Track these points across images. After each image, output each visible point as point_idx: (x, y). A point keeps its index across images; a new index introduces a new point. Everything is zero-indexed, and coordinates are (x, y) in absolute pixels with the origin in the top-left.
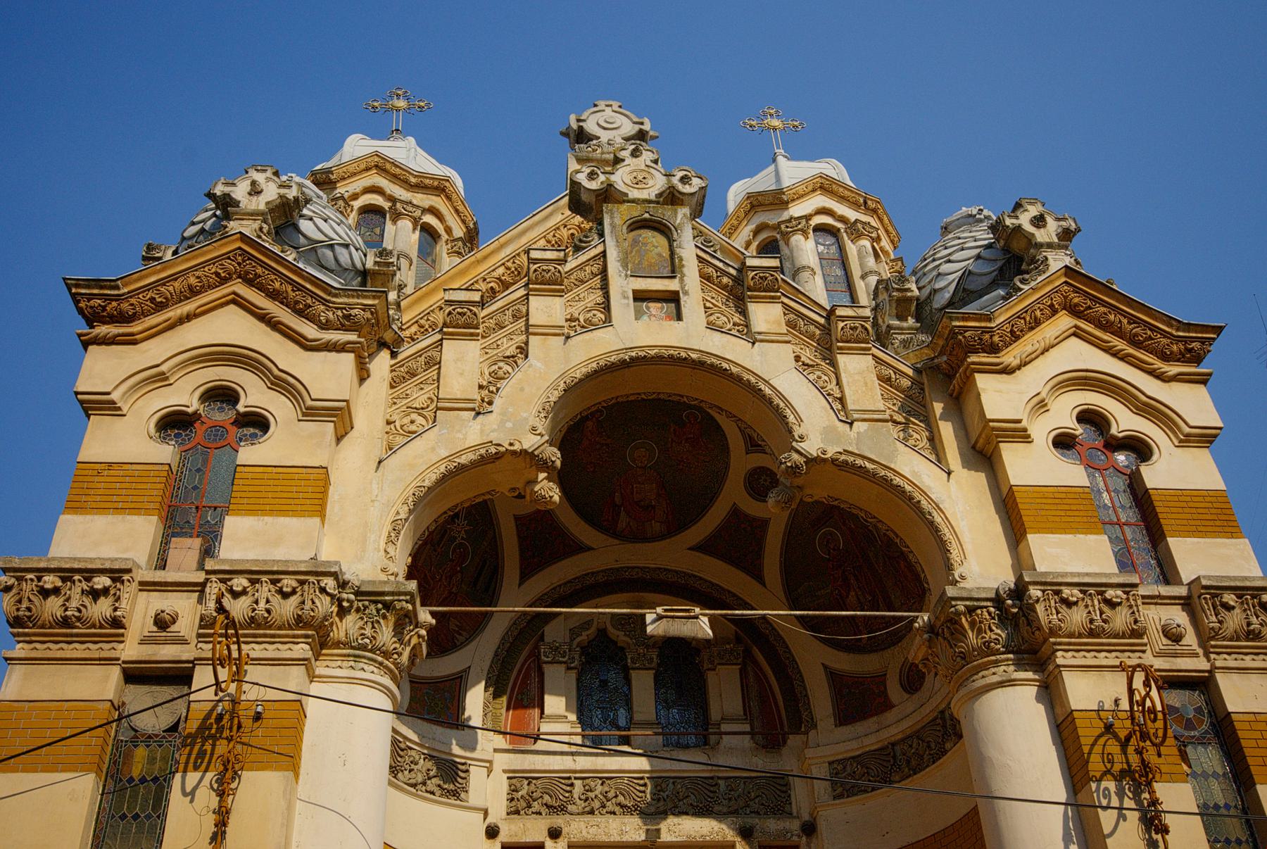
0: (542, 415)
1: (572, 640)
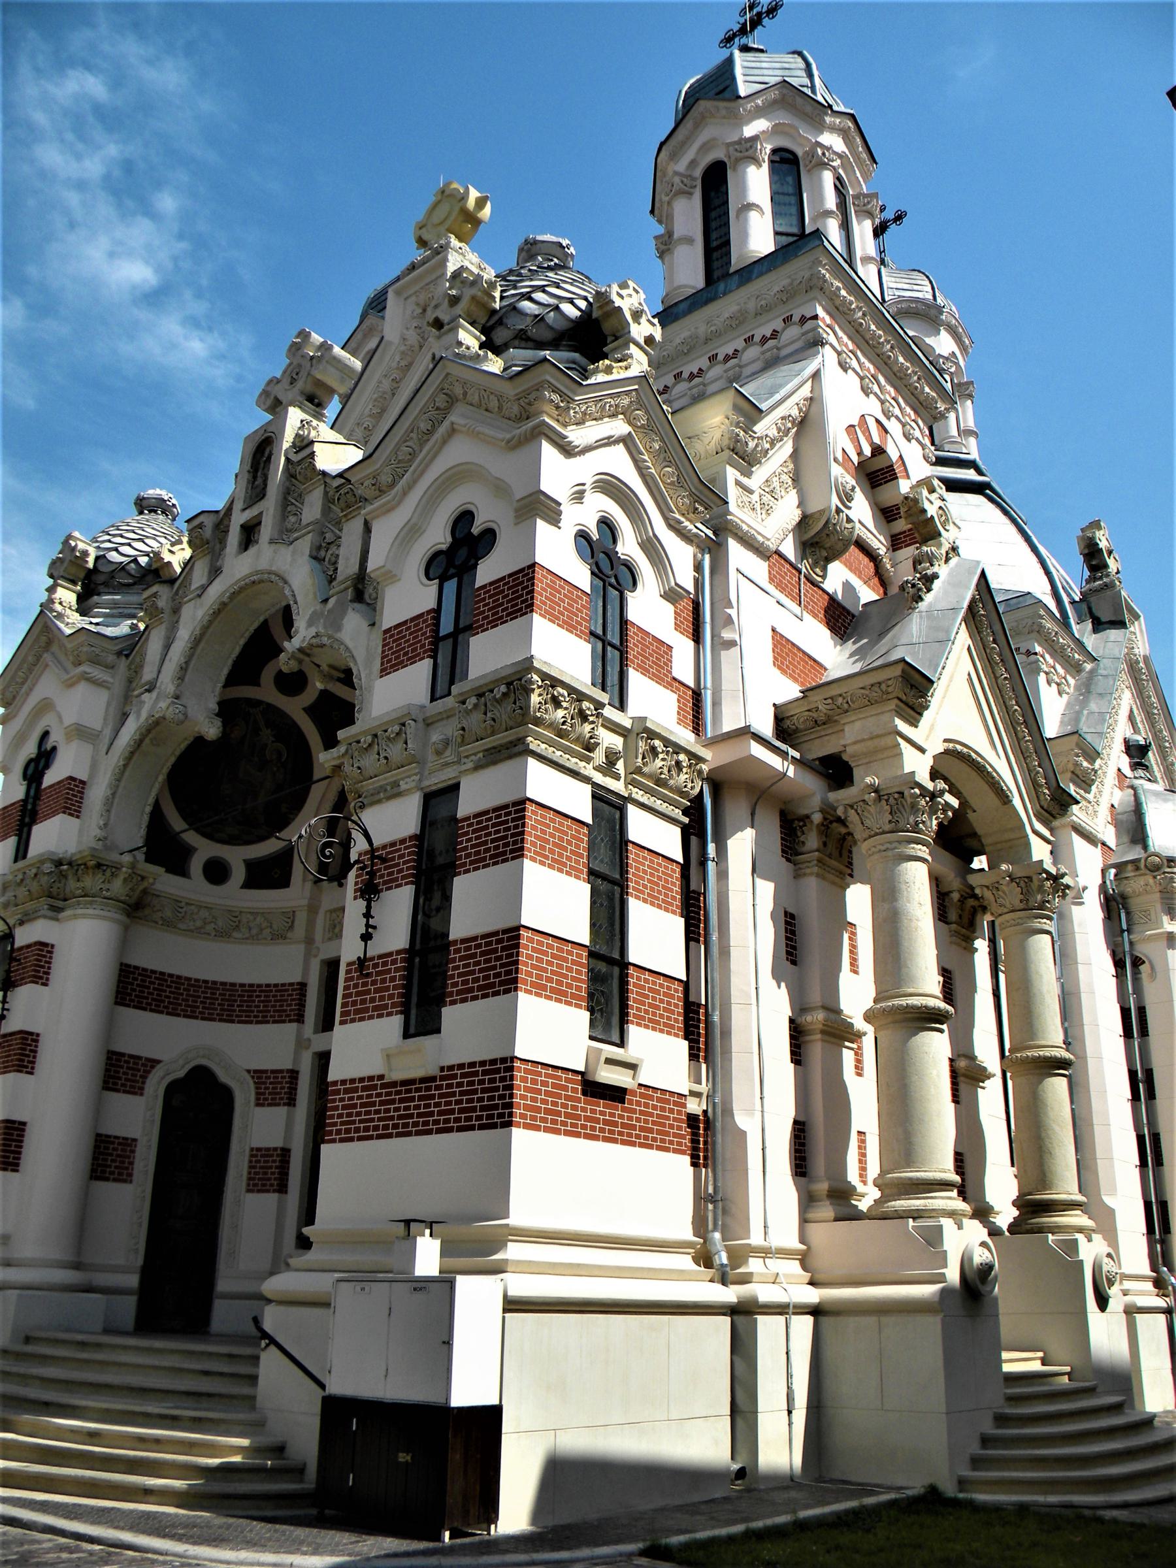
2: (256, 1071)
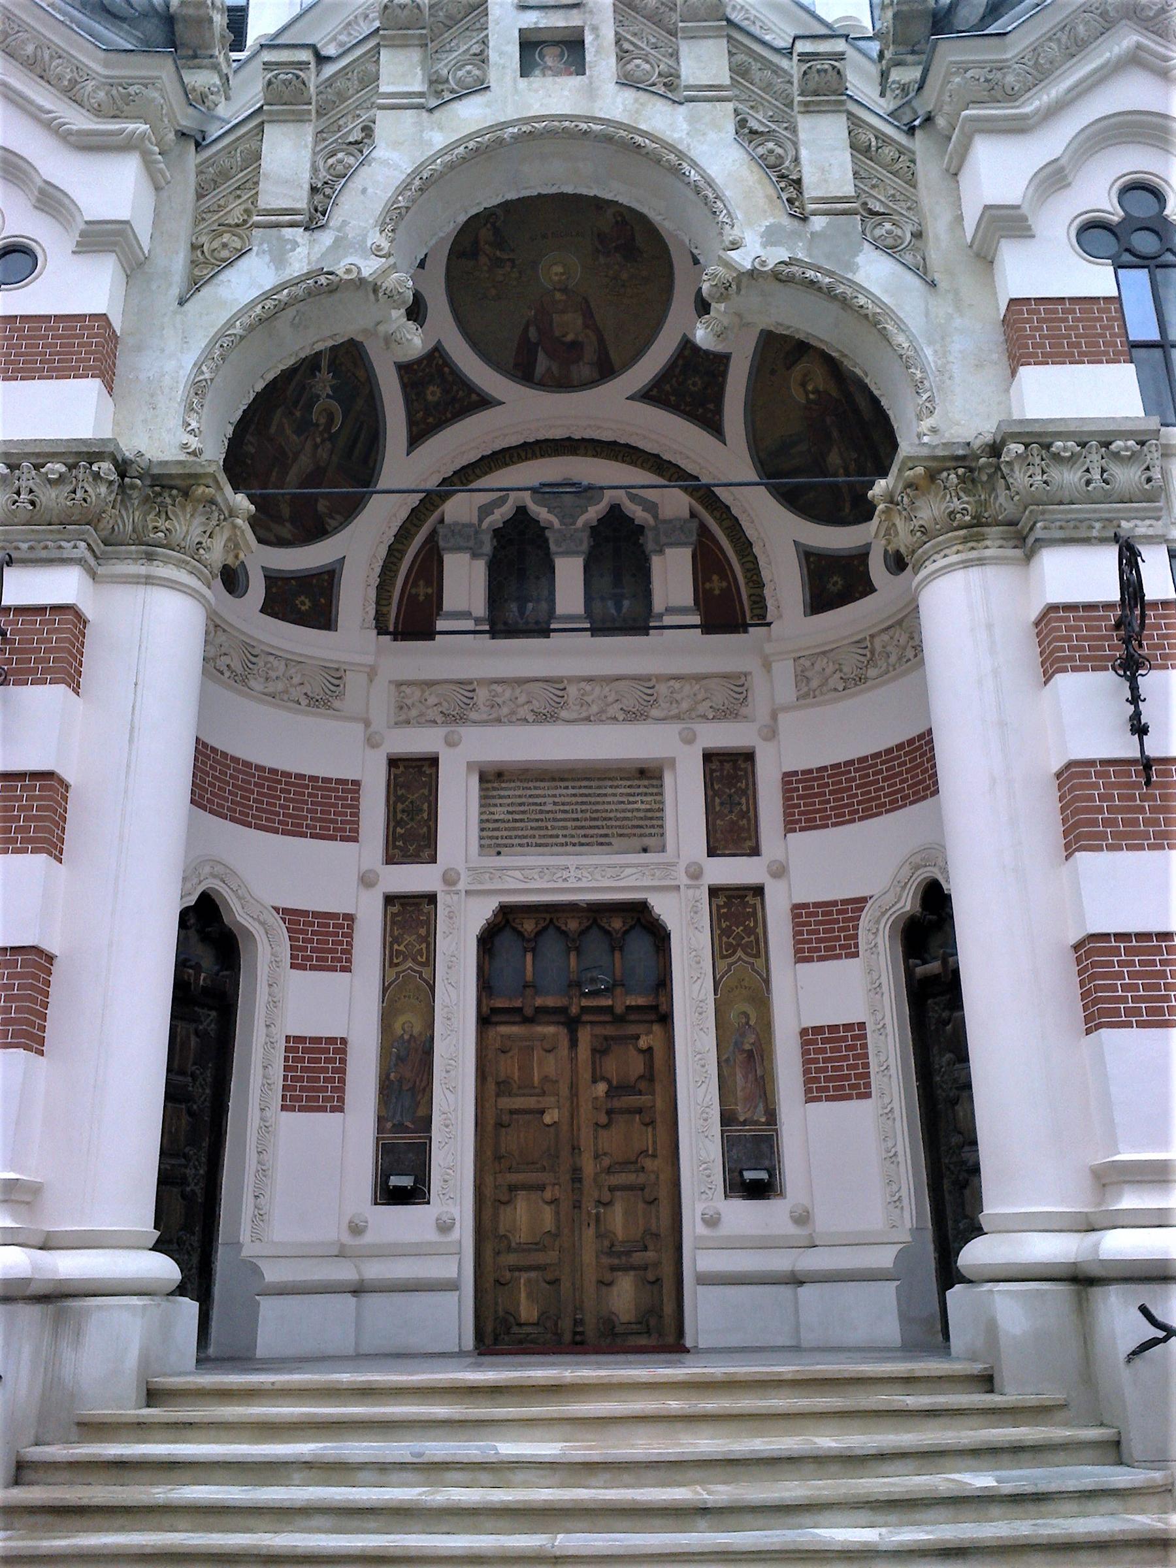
0: (390, 227)
1: (481, 521)
2: (286, 911)
